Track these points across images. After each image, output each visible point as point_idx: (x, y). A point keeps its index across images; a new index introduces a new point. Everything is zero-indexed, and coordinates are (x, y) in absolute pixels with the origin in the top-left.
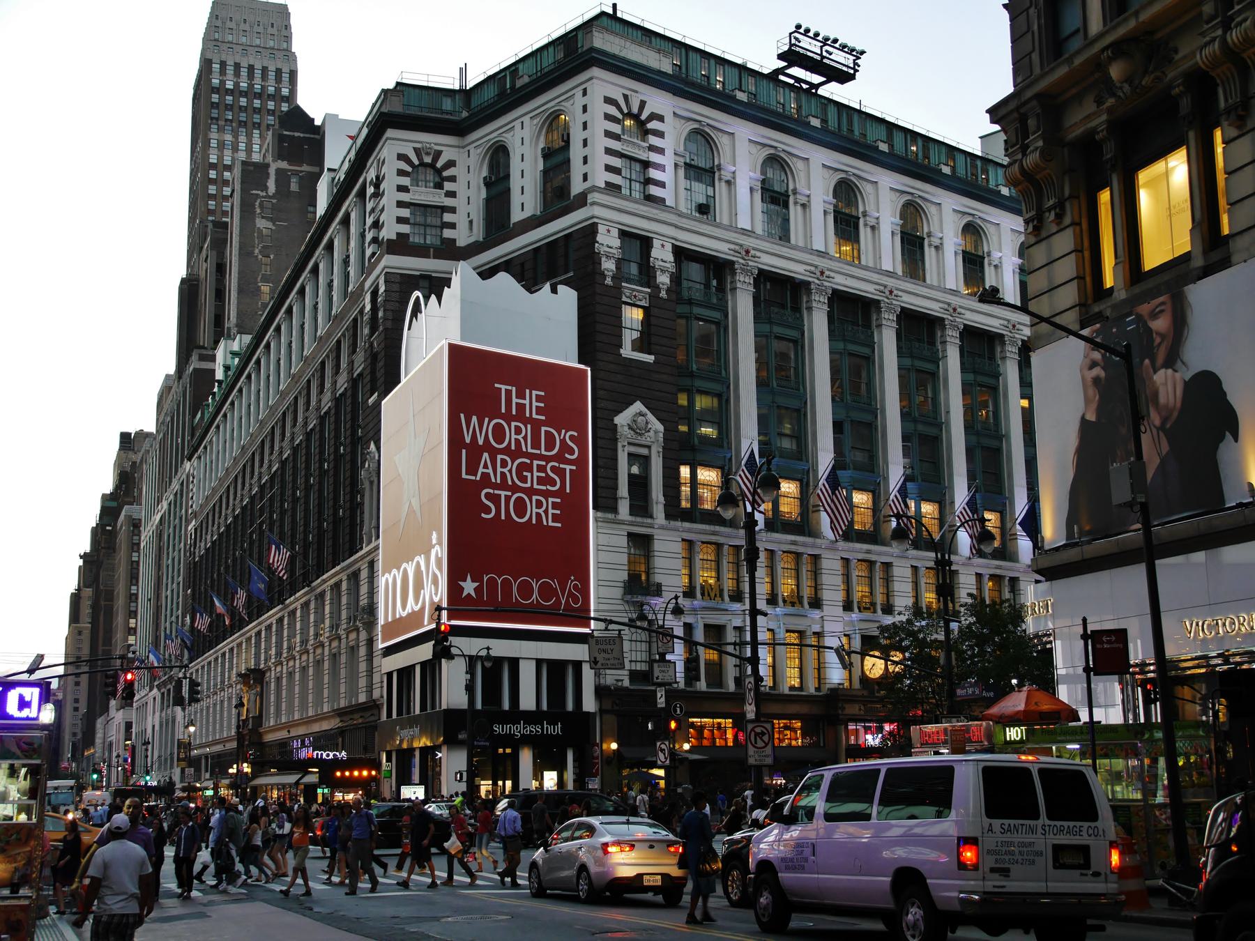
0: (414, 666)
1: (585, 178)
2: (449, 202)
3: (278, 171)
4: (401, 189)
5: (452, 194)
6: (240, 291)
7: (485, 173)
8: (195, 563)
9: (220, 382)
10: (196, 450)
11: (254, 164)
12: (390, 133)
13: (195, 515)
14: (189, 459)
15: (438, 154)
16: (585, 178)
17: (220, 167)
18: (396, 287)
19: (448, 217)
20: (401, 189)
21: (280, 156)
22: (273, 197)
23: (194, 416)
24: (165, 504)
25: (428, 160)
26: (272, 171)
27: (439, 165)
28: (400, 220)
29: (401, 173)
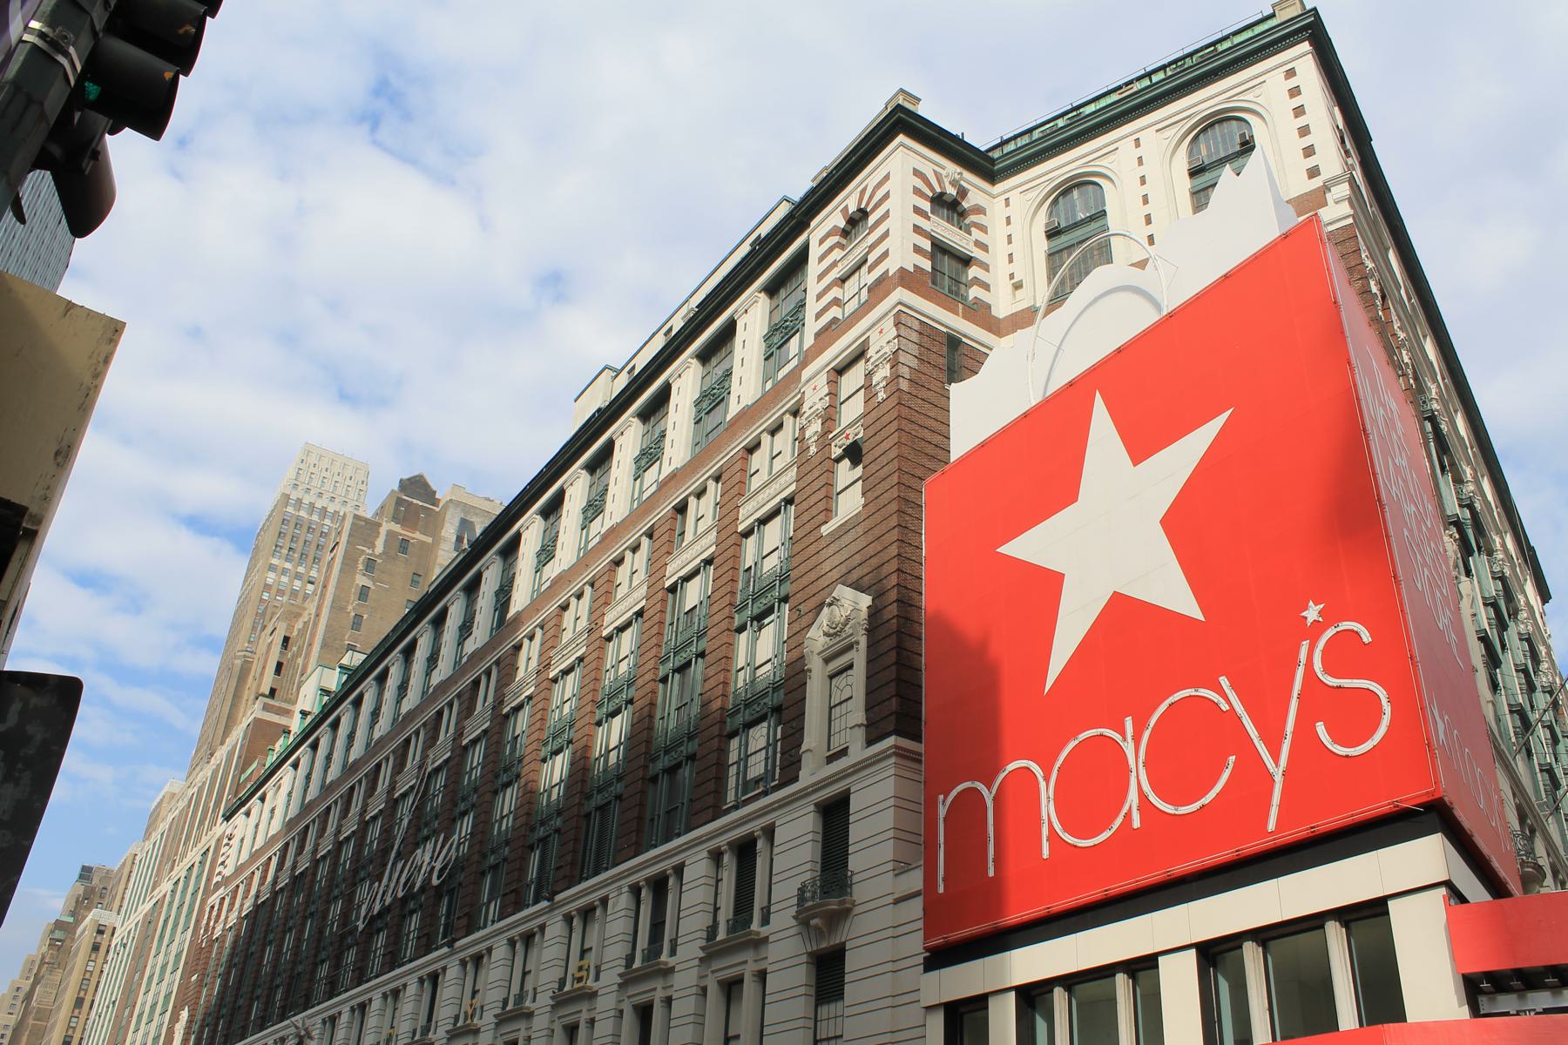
0: (1143, 967)
1: (1313, 172)
2: (976, 253)
3: (390, 533)
4: (917, 210)
5: (984, 247)
6: (324, 645)
7: (1042, 220)
8: (211, 942)
9: (304, 714)
10: (243, 804)
11: (366, 520)
12: (901, 138)
13: (226, 881)
14: (227, 818)
15: (963, 193)
16: (1313, 172)
17: (274, 591)
18: (914, 337)
19: (973, 272)
20: (917, 210)
21: (395, 519)
22: (379, 556)
23: (243, 771)
24: (166, 887)
25: (951, 191)
26: (383, 531)
27: (965, 205)
28: (918, 249)
29: (917, 191)
